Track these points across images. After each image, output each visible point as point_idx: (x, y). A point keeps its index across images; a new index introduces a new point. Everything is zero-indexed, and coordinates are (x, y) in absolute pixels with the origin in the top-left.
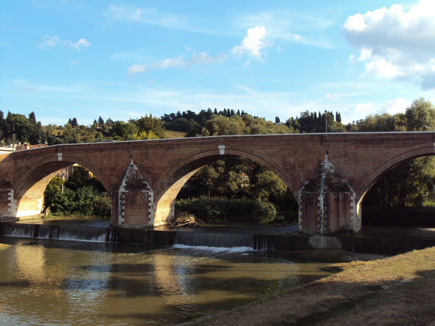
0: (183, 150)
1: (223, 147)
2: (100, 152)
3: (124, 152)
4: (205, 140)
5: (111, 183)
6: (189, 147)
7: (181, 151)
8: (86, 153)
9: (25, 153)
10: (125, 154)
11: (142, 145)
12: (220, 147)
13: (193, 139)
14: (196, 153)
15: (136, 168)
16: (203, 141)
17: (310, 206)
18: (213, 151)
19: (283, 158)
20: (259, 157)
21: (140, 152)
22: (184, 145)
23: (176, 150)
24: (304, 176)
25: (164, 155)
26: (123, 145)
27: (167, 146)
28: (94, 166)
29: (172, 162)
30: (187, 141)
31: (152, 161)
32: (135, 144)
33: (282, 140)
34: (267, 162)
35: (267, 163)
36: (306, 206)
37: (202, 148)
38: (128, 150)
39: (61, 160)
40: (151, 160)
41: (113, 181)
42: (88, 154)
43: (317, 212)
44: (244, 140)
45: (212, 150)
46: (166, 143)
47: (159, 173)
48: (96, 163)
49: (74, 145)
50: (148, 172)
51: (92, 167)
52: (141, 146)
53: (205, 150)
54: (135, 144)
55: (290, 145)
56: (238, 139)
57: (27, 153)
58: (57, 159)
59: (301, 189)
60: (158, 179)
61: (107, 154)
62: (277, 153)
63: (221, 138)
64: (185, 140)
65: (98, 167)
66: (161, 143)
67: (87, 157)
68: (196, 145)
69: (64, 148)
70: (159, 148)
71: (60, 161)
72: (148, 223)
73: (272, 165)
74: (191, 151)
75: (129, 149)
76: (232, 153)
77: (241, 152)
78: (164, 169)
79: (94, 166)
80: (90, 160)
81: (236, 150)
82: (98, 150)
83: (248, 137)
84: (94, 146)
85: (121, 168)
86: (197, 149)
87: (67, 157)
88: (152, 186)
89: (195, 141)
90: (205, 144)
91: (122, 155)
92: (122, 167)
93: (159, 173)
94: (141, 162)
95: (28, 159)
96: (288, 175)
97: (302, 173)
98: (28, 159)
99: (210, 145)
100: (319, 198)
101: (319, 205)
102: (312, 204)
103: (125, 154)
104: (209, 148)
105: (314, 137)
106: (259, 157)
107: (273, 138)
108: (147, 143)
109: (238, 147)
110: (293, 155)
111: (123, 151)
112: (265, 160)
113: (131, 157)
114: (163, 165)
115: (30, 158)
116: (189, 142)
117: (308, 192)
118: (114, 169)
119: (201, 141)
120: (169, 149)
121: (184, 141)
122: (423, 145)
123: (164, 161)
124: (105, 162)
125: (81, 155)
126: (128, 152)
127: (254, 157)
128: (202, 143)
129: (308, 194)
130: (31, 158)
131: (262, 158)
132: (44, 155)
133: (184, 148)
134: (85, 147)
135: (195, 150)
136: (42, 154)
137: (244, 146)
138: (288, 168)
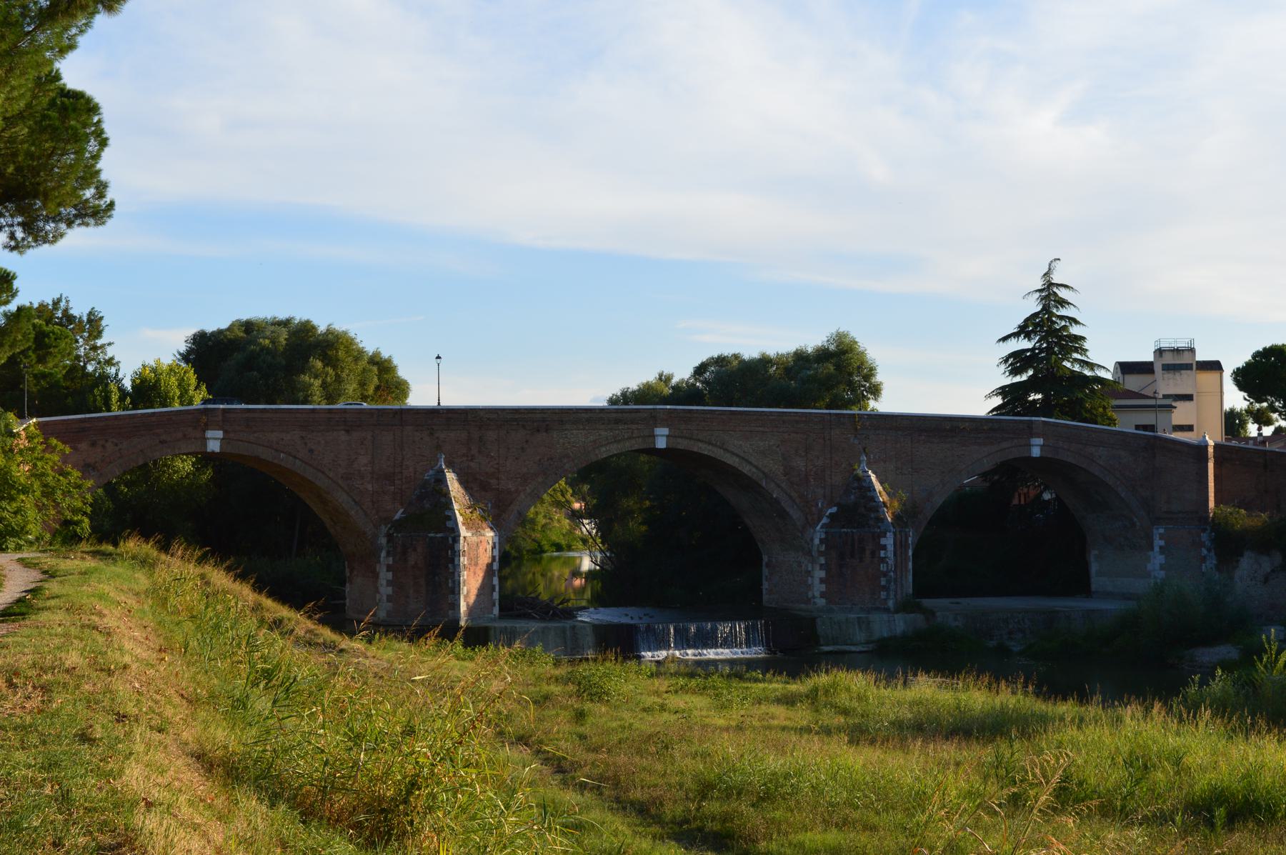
0: (572, 434)
1: (665, 431)
2: (347, 431)
6: (587, 428)
10: (422, 439)
14: (604, 443)
16: (620, 415)
18: (640, 440)
20: (737, 455)
24: (824, 497)
27: (535, 424)
28: (330, 470)
30: (583, 415)
31: (495, 459)
33: (784, 422)
34: (756, 467)
35: (754, 470)
38: (433, 429)
39: (217, 450)
44: (708, 418)
45: (639, 437)
46: (530, 415)
49: (265, 409)
51: (323, 472)
53: (624, 436)
55: (797, 433)
56: (695, 415)
58: (205, 446)
59: (820, 524)
60: (511, 503)
62: (774, 448)
63: (662, 411)
64: (577, 413)
67: (306, 444)
68: (603, 424)
71: (213, 453)
72: (492, 613)
73: (764, 473)
74: (592, 438)
76: (683, 444)
77: (700, 445)
79: (330, 470)
81: (691, 439)
83: (717, 413)
85: (412, 474)
89: (601, 415)
91: (414, 442)
92: (415, 474)
94: (467, 460)
95: (93, 444)
98: (93, 444)
99: (636, 426)
100: (883, 541)
101: (885, 554)
103: (422, 439)
104: (632, 433)
105: (842, 419)
106: (737, 455)
107: (765, 417)
109: (696, 432)
110: (803, 454)
111: (417, 431)
112: (750, 463)
117: (849, 530)
119: (614, 415)
120: (538, 431)
121: (574, 413)
128: (617, 421)
129: (846, 533)
130: (107, 441)
131: (746, 458)
133: (574, 431)
135: (600, 435)
137: (708, 430)
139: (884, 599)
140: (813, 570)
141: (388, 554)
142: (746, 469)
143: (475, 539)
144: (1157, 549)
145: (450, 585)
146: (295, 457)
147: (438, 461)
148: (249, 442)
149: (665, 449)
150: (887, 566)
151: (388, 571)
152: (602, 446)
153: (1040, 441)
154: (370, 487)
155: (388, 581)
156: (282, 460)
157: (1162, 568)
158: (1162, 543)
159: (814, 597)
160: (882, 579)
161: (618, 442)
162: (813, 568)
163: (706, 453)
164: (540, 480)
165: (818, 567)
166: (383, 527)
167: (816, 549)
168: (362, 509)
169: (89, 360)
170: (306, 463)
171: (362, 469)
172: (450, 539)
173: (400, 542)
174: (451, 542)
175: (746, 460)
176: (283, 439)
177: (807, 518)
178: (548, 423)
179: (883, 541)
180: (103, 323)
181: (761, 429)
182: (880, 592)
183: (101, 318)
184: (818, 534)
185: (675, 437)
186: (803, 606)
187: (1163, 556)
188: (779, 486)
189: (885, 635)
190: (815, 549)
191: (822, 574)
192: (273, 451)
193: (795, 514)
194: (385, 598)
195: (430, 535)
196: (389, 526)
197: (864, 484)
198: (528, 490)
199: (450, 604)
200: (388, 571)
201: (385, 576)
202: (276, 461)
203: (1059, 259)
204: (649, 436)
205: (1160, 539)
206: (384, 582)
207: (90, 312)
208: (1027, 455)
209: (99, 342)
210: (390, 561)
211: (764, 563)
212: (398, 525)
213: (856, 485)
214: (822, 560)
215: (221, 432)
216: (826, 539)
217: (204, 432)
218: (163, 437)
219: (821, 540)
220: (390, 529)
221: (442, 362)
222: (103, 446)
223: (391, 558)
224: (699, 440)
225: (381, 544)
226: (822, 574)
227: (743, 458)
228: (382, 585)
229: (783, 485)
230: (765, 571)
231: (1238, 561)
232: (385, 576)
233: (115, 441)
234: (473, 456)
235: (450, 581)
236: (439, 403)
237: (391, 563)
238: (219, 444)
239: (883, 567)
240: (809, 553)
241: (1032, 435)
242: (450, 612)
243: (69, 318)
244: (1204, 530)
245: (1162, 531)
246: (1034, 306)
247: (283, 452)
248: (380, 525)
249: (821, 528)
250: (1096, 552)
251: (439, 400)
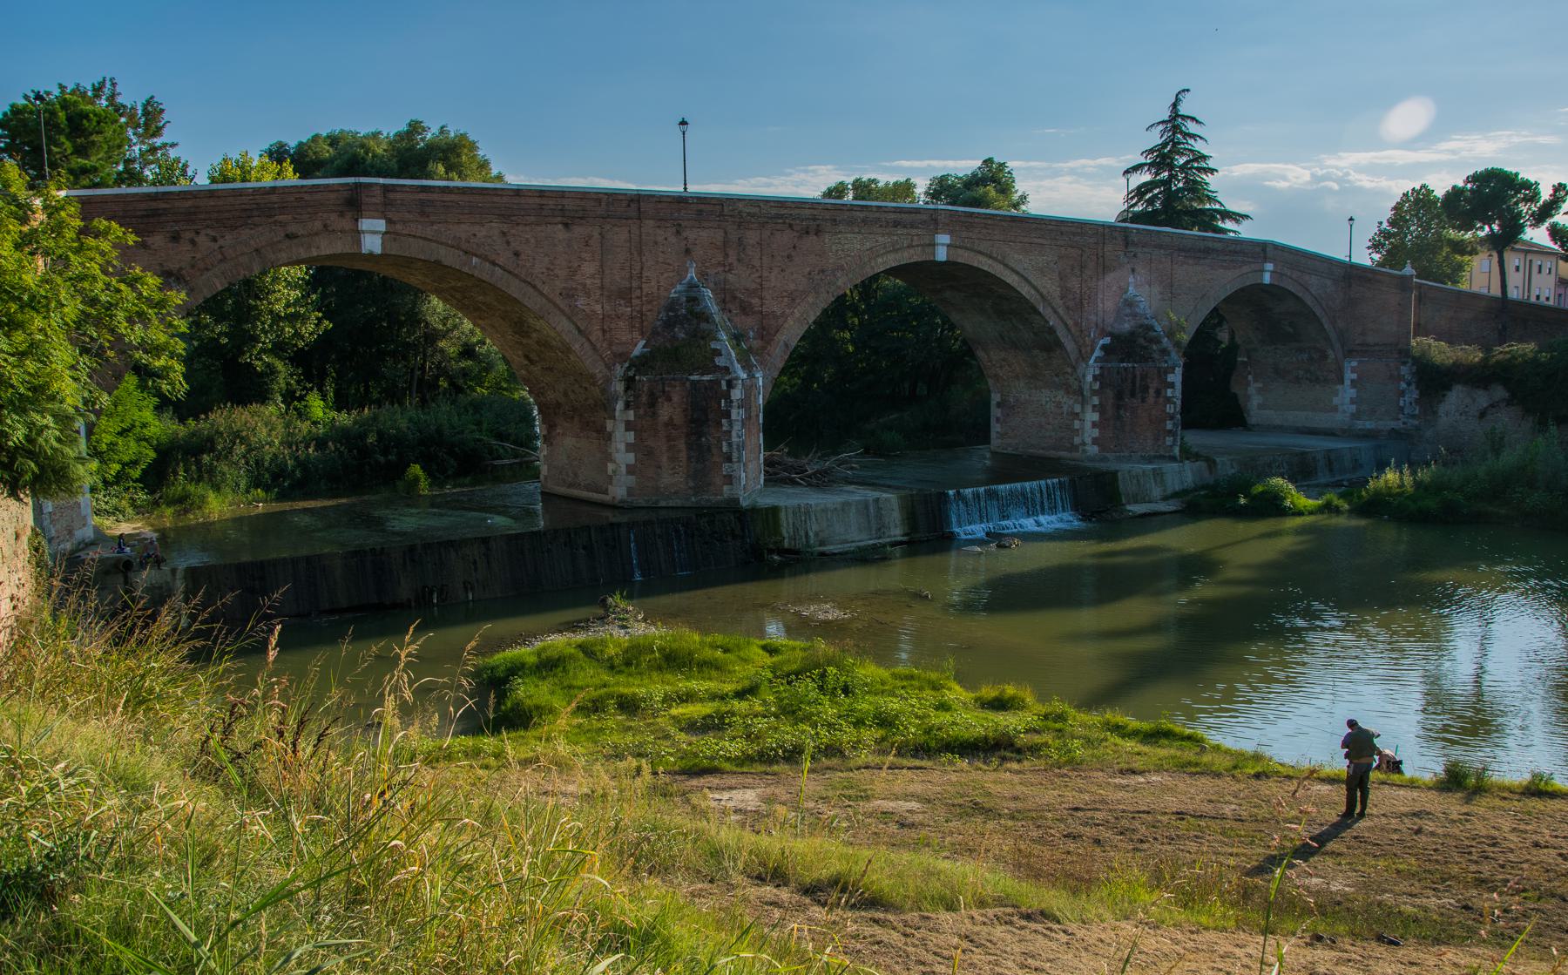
0: (846, 239)
2: (566, 225)
3: (659, 231)
4: (903, 215)
5: (614, 348)
6: (863, 231)
7: (843, 242)
8: (505, 227)
9: (154, 205)
10: (666, 239)
11: (726, 211)
13: (874, 209)
17: (1133, 395)
19: (1061, 279)
20: (1017, 273)
22: (851, 223)
23: (827, 238)
25: (793, 254)
26: (660, 206)
29: (818, 277)
32: (702, 207)
33: (1062, 233)
34: (1035, 288)
35: (1033, 292)
36: (1119, 396)
37: (895, 238)
38: (680, 225)
39: (378, 250)
40: (754, 267)
41: (624, 339)
42: (513, 231)
43: (1165, 411)
45: (918, 246)
46: (797, 211)
47: (778, 313)
48: (548, 269)
50: (745, 309)
51: (534, 287)
54: (702, 207)
56: (976, 220)
57: (162, 205)
58: (359, 243)
59: (1093, 358)
61: (596, 234)
62: (1052, 264)
66: (783, 211)
67: (508, 243)
68: (881, 226)
69: (391, 196)
70: (779, 227)
71: (371, 255)
74: (868, 245)
75: (684, 224)
76: (964, 257)
77: (982, 258)
80: (523, 257)
81: (972, 250)
82: (559, 219)
84: (538, 201)
85: (655, 290)
87: (411, 239)
89: (877, 215)
90: (905, 227)
91: (656, 243)
92: (658, 289)
93: (778, 313)
95: (176, 238)
96: (1070, 322)
100: (1170, 378)
102: (1145, 389)
106: (1017, 273)
108: (740, 205)
111: (659, 227)
113: (688, 251)
114: (792, 287)
115: (188, 235)
116: (861, 215)
117: (1130, 365)
118: (625, 295)
119: (892, 216)
120: (807, 233)
122: (1253, 266)
123: (792, 274)
124: (589, 268)
125: (482, 232)
126: (678, 232)
127: (1007, 272)
128: (896, 224)
129: (1126, 369)
130: (198, 233)
132: (283, 225)
134: (496, 199)
136: (270, 216)
139: (1171, 446)
140: (1083, 411)
141: (627, 406)
142: (1025, 290)
144: (1347, 382)
145: (725, 449)
146: (494, 263)
147: (687, 272)
148: (425, 239)
149: (945, 262)
150: (1175, 408)
151: (627, 429)
152: (878, 256)
153: (1269, 266)
154: (598, 308)
155: (628, 445)
156: (475, 267)
157: (1352, 401)
158: (1354, 376)
159: (1084, 444)
160: (1168, 422)
161: (896, 251)
162: (1083, 408)
163: (986, 269)
164: (810, 300)
165: (1089, 408)
166: (618, 367)
167: (1088, 387)
168: (589, 340)
169: (147, 163)
170: (510, 272)
171: (588, 282)
172: (724, 383)
173: (645, 389)
174: (725, 388)
175: (1026, 279)
176: (475, 235)
177: (1080, 351)
178: (818, 222)
179: (1170, 378)
180: (166, 116)
181: (1040, 241)
182: (1164, 438)
183: (162, 111)
184: (1090, 370)
185: (956, 247)
186: (1063, 454)
187: (1353, 391)
188: (1056, 312)
189: (1177, 489)
190: (1086, 387)
191: (1096, 417)
192: (461, 253)
193: (1070, 345)
194: (623, 469)
195: (692, 378)
196: (627, 365)
197: (1138, 310)
198: (797, 315)
199: (725, 476)
200: (627, 429)
201: (622, 438)
202: (466, 269)
203: (1188, 90)
204: (929, 245)
205: (1352, 372)
206: (622, 447)
207: (148, 103)
208: (1259, 281)
209: (158, 141)
210: (631, 415)
211: (993, 403)
212: (642, 364)
213: (1128, 311)
214: (1096, 401)
215: (383, 222)
216: (1101, 375)
217: (357, 220)
218: (292, 228)
219: (1094, 376)
220: (629, 369)
221: (690, 130)
222: (193, 242)
223: (632, 412)
224: (980, 252)
225: (615, 391)
226: (1096, 417)
227: (1022, 276)
228: (617, 451)
229: (1061, 311)
230: (995, 412)
231: (1444, 396)
232: (622, 438)
233: (213, 233)
234: (730, 264)
235: (724, 443)
236: (685, 189)
237: (632, 418)
238: (380, 241)
239: (1170, 409)
240: (1080, 392)
241: (1265, 260)
242: (725, 488)
243: (119, 109)
244: (1404, 363)
245: (1354, 364)
246: (1155, 138)
247: (476, 256)
248: (614, 365)
249: (1095, 361)
250: (1260, 385)
251: (685, 184)
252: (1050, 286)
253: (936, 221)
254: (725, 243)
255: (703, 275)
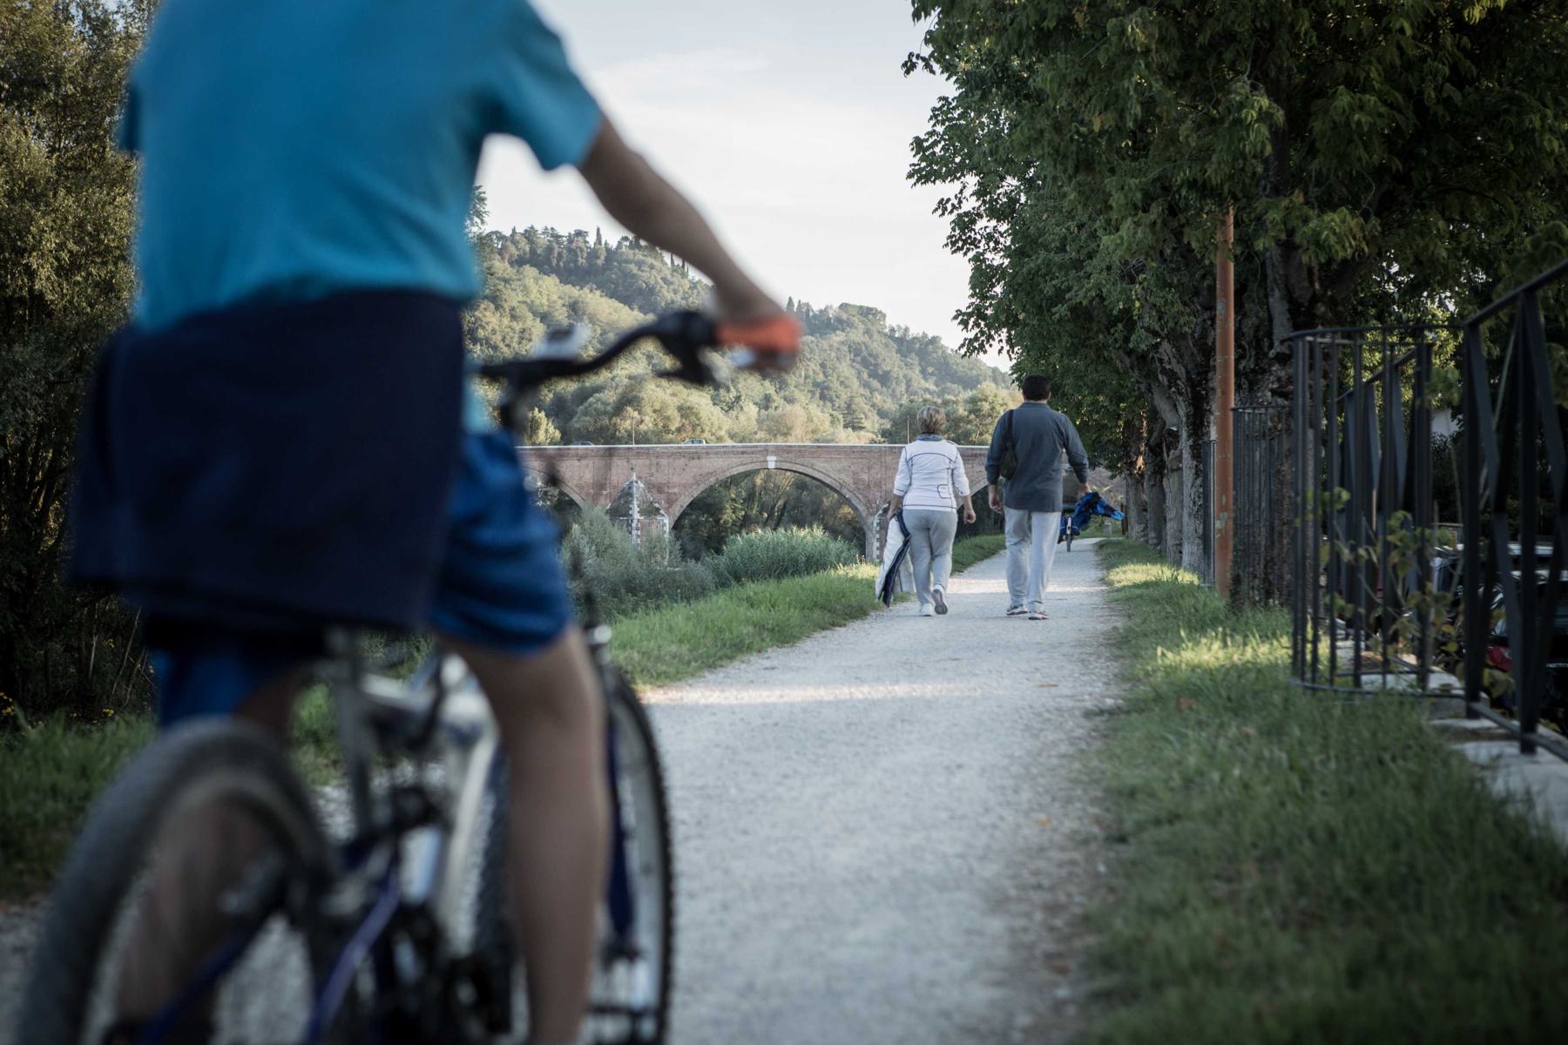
1: (774, 458)
12: (769, 458)
15: (642, 485)
21: (648, 462)
22: (716, 453)
50: (660, 491)
52: (648, 453)
65: (575, 482)
78: (685, 486)
86: (735, 460)
88: (667, 510)
96: (860, 496)
97: (879, 494)
113: (632, 469)
114: (684, 481)
128: (743, 453)
138: (861, 487)
143: (647, 521)
219: (878, 524)
252: (847, 479)
253: (767, 451)
254: (651, 465)
255: (639, 478)
